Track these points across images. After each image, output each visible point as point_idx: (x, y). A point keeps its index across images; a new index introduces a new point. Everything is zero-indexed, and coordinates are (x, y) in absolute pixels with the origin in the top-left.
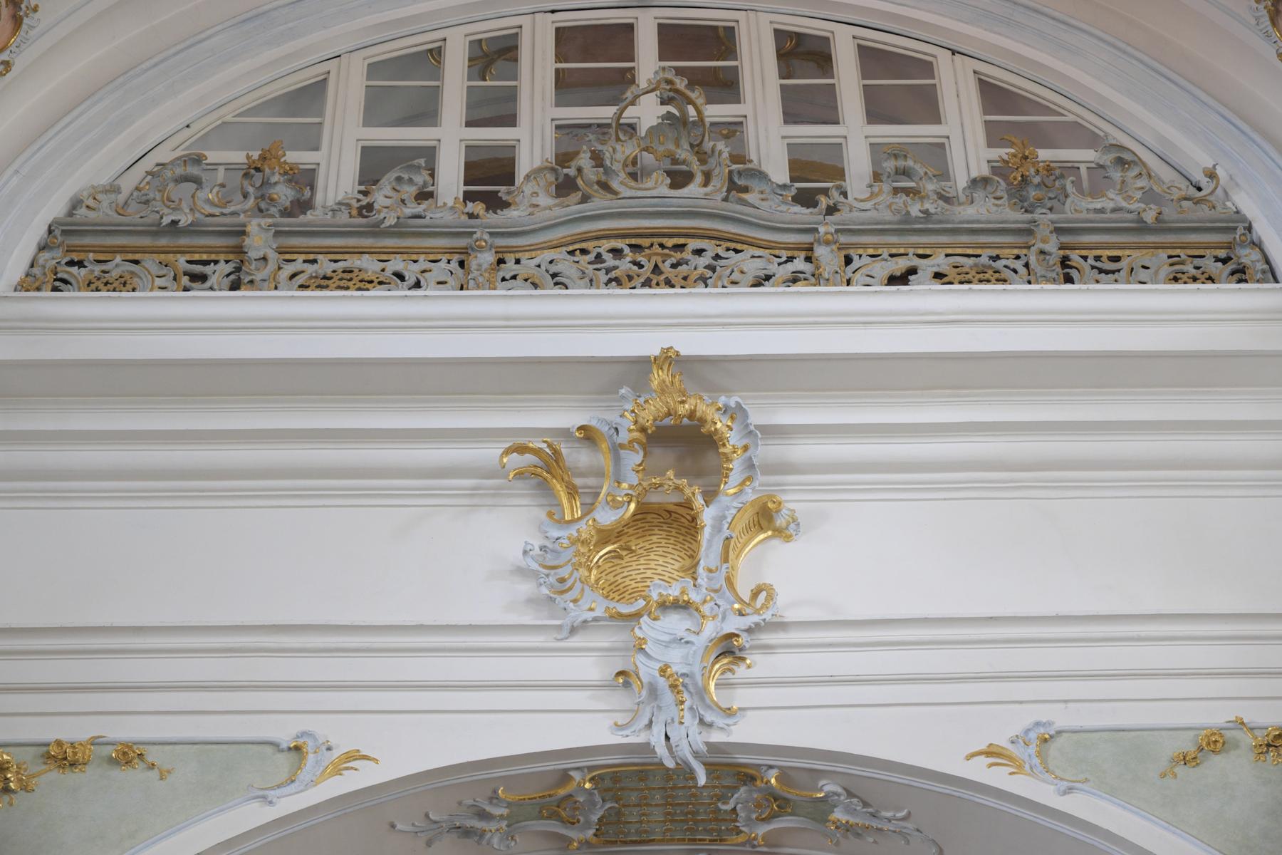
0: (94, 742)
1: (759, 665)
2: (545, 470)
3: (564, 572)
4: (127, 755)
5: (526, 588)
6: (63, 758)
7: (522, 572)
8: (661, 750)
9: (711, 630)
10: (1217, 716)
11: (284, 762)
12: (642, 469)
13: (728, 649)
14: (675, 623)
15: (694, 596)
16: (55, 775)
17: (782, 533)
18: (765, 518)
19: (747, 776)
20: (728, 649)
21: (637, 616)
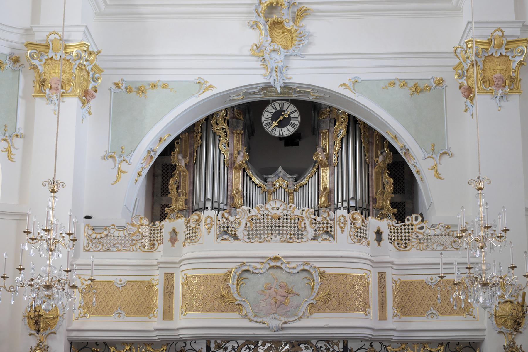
0: (159, 81)
6: (154, 86)
10: (392, 77)
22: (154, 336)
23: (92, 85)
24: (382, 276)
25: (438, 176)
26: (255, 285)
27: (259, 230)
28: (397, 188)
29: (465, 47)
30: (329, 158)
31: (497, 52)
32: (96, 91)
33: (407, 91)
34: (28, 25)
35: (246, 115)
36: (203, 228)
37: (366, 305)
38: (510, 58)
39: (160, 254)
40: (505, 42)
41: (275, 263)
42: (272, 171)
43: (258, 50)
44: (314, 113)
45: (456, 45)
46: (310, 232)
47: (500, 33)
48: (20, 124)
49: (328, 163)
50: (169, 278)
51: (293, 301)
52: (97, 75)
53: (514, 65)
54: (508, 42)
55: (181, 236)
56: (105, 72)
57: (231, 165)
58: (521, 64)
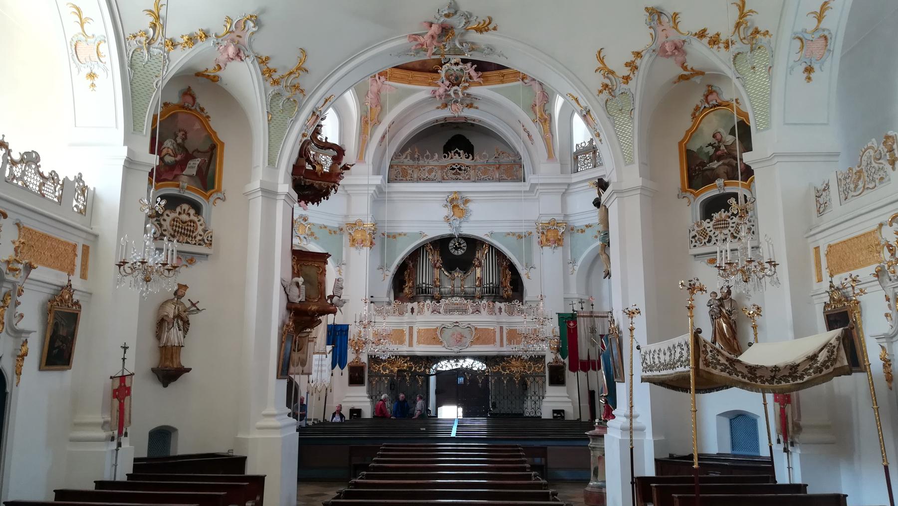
22: (405, 353)
24: (501, 328)
25: (528, 278)
26: (448, 333)
27: (449, 311)
28: (510, 286)
30: (480, 263)
33: (515, 238)
35: (441, 244)
36: (426, 308)
37: (495, 341)
39: (407, 317)
41: (456, 324)
42: (454, 269)
43: (447, 219)
44: (473, 243)
46: (471, 310)
48: (344, 259)
49: (480, 265)
50: (411, 329)
51: (464, 340)
55: (416, 310)
57: (435, 266)
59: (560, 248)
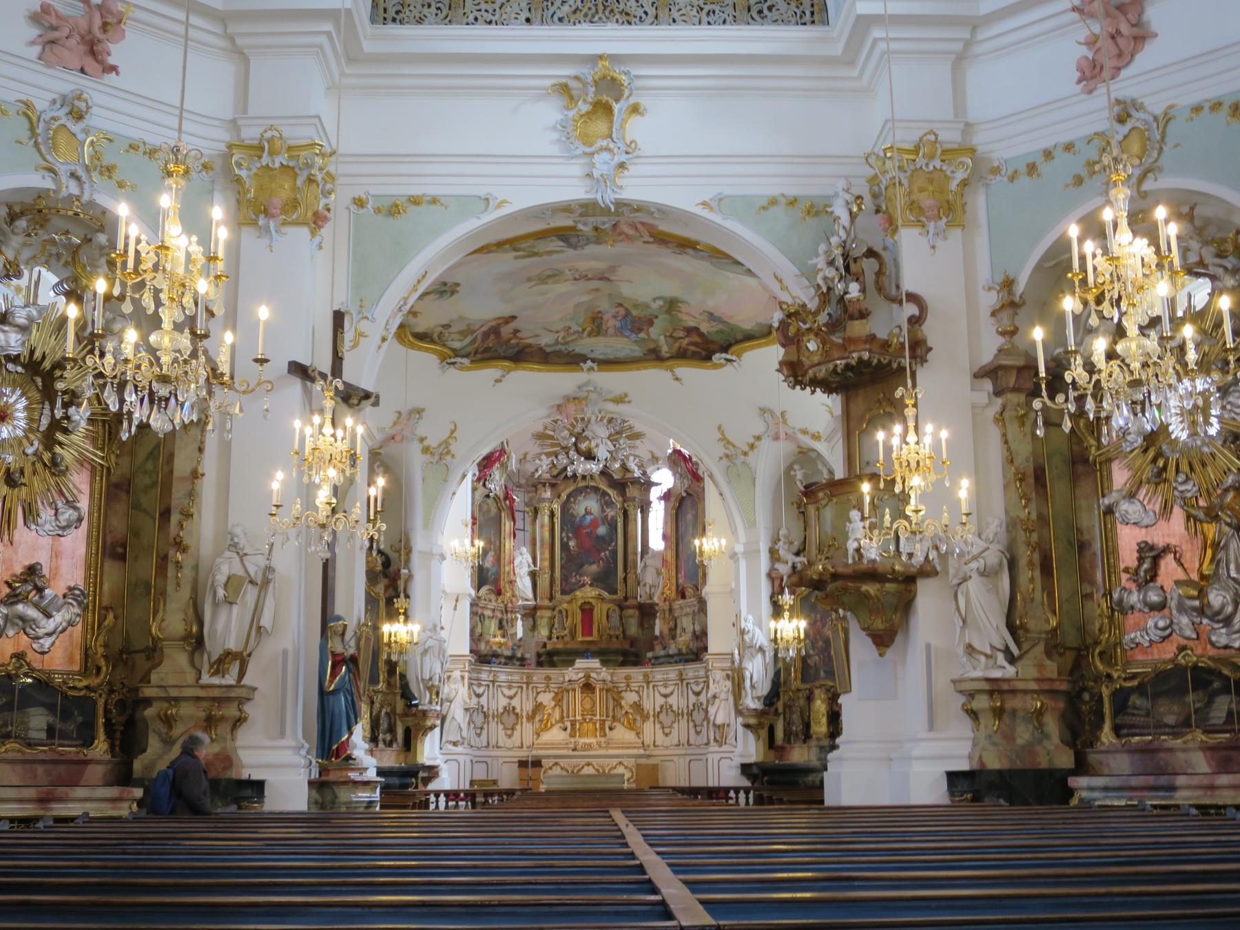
1: (633, 170)
2: (563, 89)
3: (569, 130)
4: (434, 201)
5: (555, 136)
6: (415, 201)
7: (554, 128)
8: (600, 201)
9: (617, 159)
10: (775, 191)
11: (483, 204)
12: (596, 93)
13: (622, 166)
14: (605, 156)
15: (612, 145)
16: (412, 209)
17: (642, 114)
18: (635, 109)
19: (626, 205)
20: (622, 166)
21: (593, 154)
23: (323, 202)
29: (882, 154)
31: (927, 165)
32: (329, 210)
34: (229, 116)
38: (948, 173)
40: (939, 152)
45: (868, 150)
47: (932, 138)
52: (329, 186)
53: (953, 185)
54: (944, 152)
56: (341, 180)
58: (964, 183)
59: (957, 232)
